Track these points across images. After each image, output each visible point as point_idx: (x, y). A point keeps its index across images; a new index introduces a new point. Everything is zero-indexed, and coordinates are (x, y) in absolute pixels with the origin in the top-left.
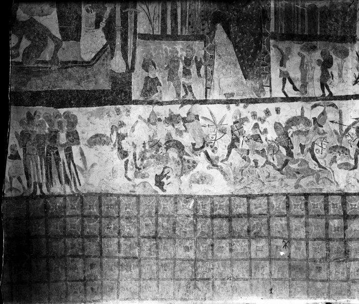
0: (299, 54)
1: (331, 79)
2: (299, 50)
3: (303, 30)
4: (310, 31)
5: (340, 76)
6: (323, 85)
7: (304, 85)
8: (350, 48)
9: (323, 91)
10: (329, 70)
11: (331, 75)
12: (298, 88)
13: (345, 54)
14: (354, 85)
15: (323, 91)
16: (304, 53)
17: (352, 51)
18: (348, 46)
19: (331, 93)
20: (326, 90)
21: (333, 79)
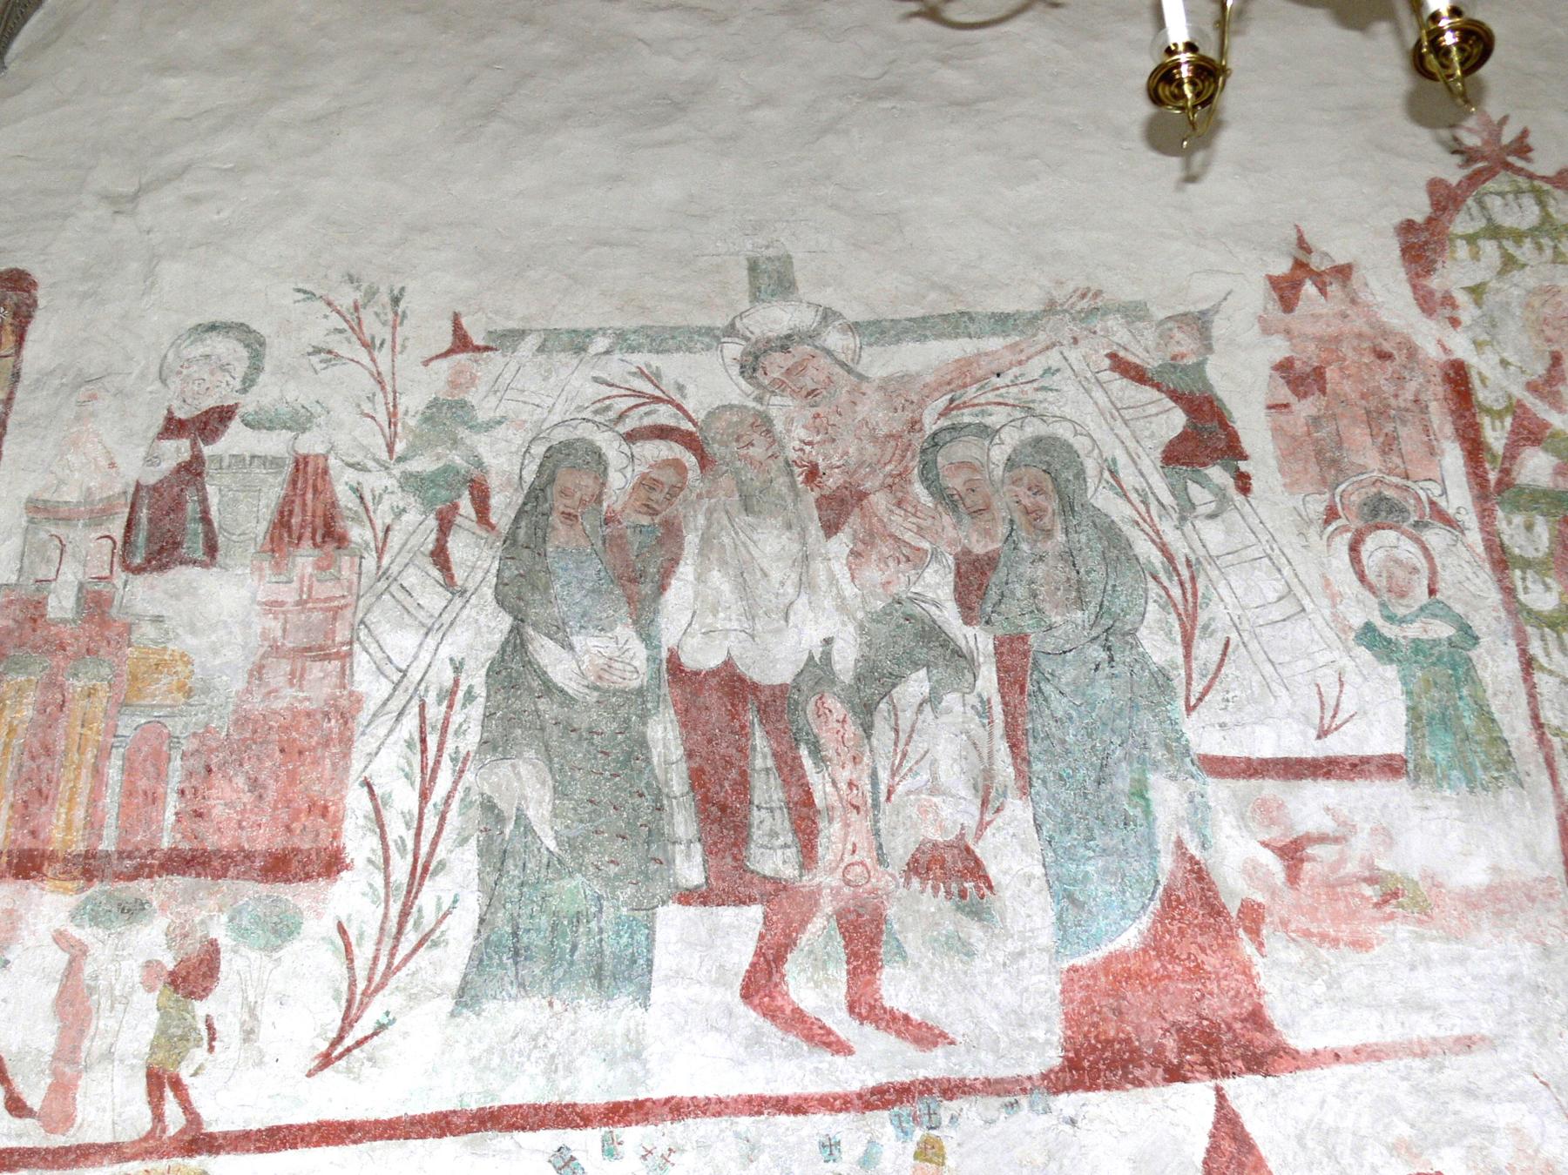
0: (60, 938)
1: (199, 1054)
2: (61, 920)
3: (94, 825)
4: (125, 831)
5: (249, 1035)
6: (160, 1082)
7: (62, 1089)
8: (304, 903)
9: (158, 1116)
10: (201, 1008)
11: (204, 1033)
12: (34, 1100)
13: (282, 930)
14: (309, 1075)
15: (158, 1116)
16: (85, 934)
17: (319, 915)
18: (296, 895)
19: (193, 1118)
20: (172, 1108)
21: (211, 1049)
